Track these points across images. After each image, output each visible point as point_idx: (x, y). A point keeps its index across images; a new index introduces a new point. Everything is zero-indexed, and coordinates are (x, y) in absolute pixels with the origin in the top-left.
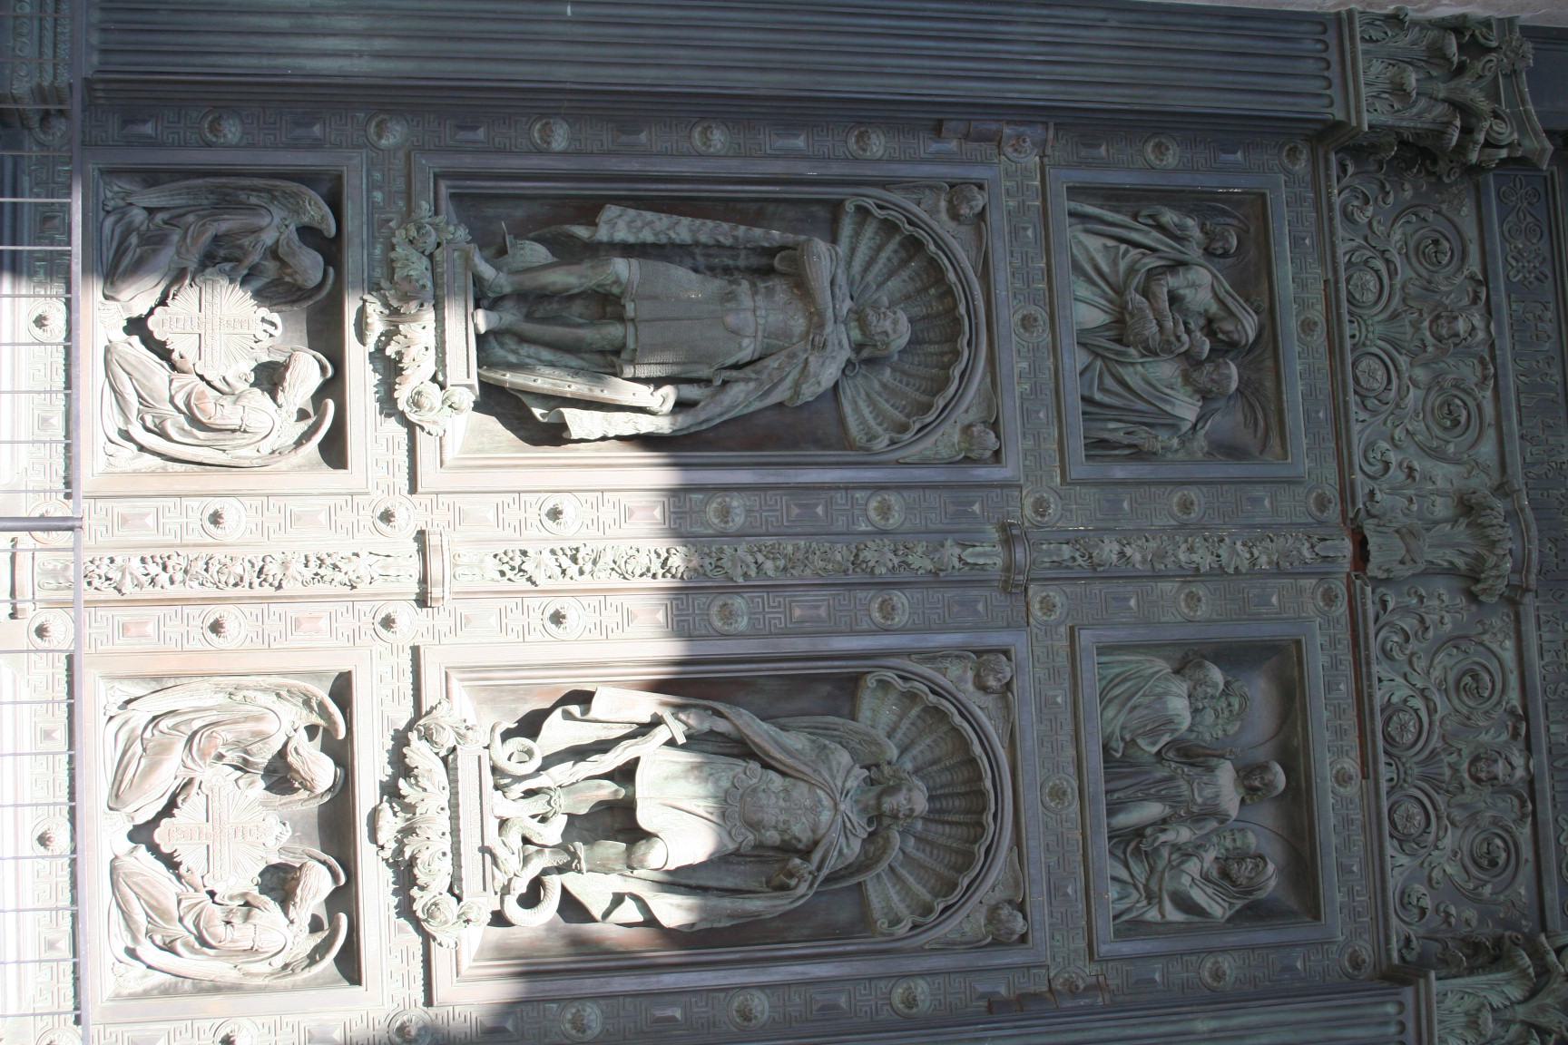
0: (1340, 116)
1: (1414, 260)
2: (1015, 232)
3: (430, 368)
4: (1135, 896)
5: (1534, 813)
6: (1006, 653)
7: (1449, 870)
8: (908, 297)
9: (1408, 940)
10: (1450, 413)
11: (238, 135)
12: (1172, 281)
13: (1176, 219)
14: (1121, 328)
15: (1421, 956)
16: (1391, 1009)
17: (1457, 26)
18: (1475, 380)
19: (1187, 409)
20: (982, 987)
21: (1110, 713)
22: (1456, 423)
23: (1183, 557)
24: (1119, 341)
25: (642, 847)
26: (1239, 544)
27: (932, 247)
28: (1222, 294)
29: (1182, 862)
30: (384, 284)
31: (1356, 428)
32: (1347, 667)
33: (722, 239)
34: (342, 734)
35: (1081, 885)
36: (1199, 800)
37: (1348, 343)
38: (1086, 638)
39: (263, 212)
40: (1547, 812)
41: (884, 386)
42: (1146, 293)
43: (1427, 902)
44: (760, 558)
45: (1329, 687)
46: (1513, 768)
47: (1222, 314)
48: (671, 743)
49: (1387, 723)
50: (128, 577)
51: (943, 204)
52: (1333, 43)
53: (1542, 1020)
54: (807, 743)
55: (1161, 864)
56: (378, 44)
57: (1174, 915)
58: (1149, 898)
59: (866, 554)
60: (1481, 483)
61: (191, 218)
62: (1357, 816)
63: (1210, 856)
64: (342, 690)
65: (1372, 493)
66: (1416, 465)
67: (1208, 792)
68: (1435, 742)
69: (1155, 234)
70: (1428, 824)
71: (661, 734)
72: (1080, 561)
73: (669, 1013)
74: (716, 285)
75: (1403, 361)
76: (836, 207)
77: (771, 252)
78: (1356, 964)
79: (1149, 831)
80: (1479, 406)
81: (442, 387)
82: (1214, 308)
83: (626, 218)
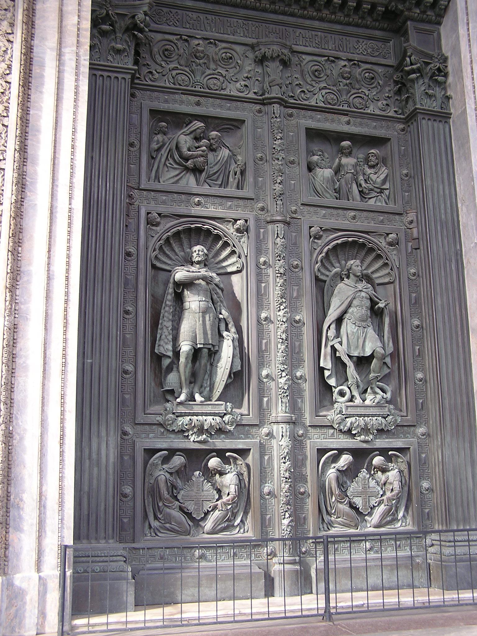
0: (130, 76)
1: (171, 60)
2: (164, 202)
3: (218, 419)
4: (380, 197)
5: (358, 61)
6: (310, 227)
7: (374, 93)
8: (181, 245)
9: (395, 111)
10: (227, 59)
11: (128, 487)
12: (185, 150)
13: (155, 143)
14: (197, 171)
15: (400, 108)
16: (424, 122)
17: (95, 23)
18: (214, 47)
19: (224, 153)
20: (410, 250)
21: (328, 195)
22: (231, 58)
23: (280, 163)
24: (201, 171)
25: (375, 354)
26: (275, 142)
27: (169, 234)
28: (188, 132)
29: (372, 180)
30: (186, 434)
31: (232, 93)
32: (313, 113)
33: (171, 310)
34: (336, 452)
35: (380, 214)
36: (353, 171)
37: (202, 90)
38: (305, 201)
39: (159, 478)
40: (356, 57)
41: (213, 257)
42: (187, 160)
43: (385, 102)
44: (282, 307)
45: (319, 121)
46: (345, 66)
47: (194, 133)
48: (341, 343)
49: (330, 104)
50: (290, 524)
51: (154, 228)
52: (100, 73)
53: (429, 75)
54: (337, 298)
55: (371, 187)
56: (103, 433)
57: (387, 186)
58: (381, 192)
59: (282, 271)
60: (251, 55)
61: (160, 504)
62: (359, 120)
63: (369, 171)
64: (322, 452)
65: (255, 93)
66: (246, 75)
67: (350, 167)
68: (335, 88)
69: (163, 151)
70: (361, 97)
71: (337, 346)
72: (281, 198)
73: (417, 351)
74: (186, 314)
75: (208, 72)
76: (154, 267)
77: (175, 292)
78: (403, 130)
79: (361, 189)
80: (224, 48)
81: (225, 414)
82: (192, 136)
83: (164, 345)
